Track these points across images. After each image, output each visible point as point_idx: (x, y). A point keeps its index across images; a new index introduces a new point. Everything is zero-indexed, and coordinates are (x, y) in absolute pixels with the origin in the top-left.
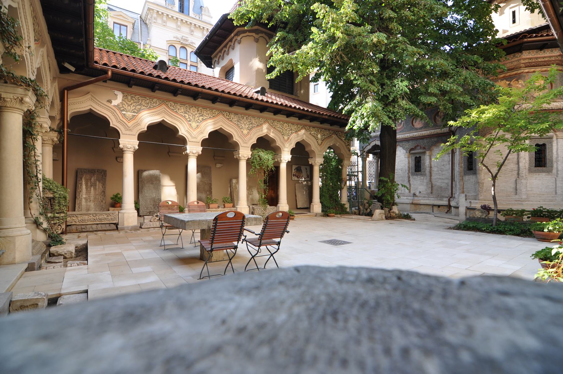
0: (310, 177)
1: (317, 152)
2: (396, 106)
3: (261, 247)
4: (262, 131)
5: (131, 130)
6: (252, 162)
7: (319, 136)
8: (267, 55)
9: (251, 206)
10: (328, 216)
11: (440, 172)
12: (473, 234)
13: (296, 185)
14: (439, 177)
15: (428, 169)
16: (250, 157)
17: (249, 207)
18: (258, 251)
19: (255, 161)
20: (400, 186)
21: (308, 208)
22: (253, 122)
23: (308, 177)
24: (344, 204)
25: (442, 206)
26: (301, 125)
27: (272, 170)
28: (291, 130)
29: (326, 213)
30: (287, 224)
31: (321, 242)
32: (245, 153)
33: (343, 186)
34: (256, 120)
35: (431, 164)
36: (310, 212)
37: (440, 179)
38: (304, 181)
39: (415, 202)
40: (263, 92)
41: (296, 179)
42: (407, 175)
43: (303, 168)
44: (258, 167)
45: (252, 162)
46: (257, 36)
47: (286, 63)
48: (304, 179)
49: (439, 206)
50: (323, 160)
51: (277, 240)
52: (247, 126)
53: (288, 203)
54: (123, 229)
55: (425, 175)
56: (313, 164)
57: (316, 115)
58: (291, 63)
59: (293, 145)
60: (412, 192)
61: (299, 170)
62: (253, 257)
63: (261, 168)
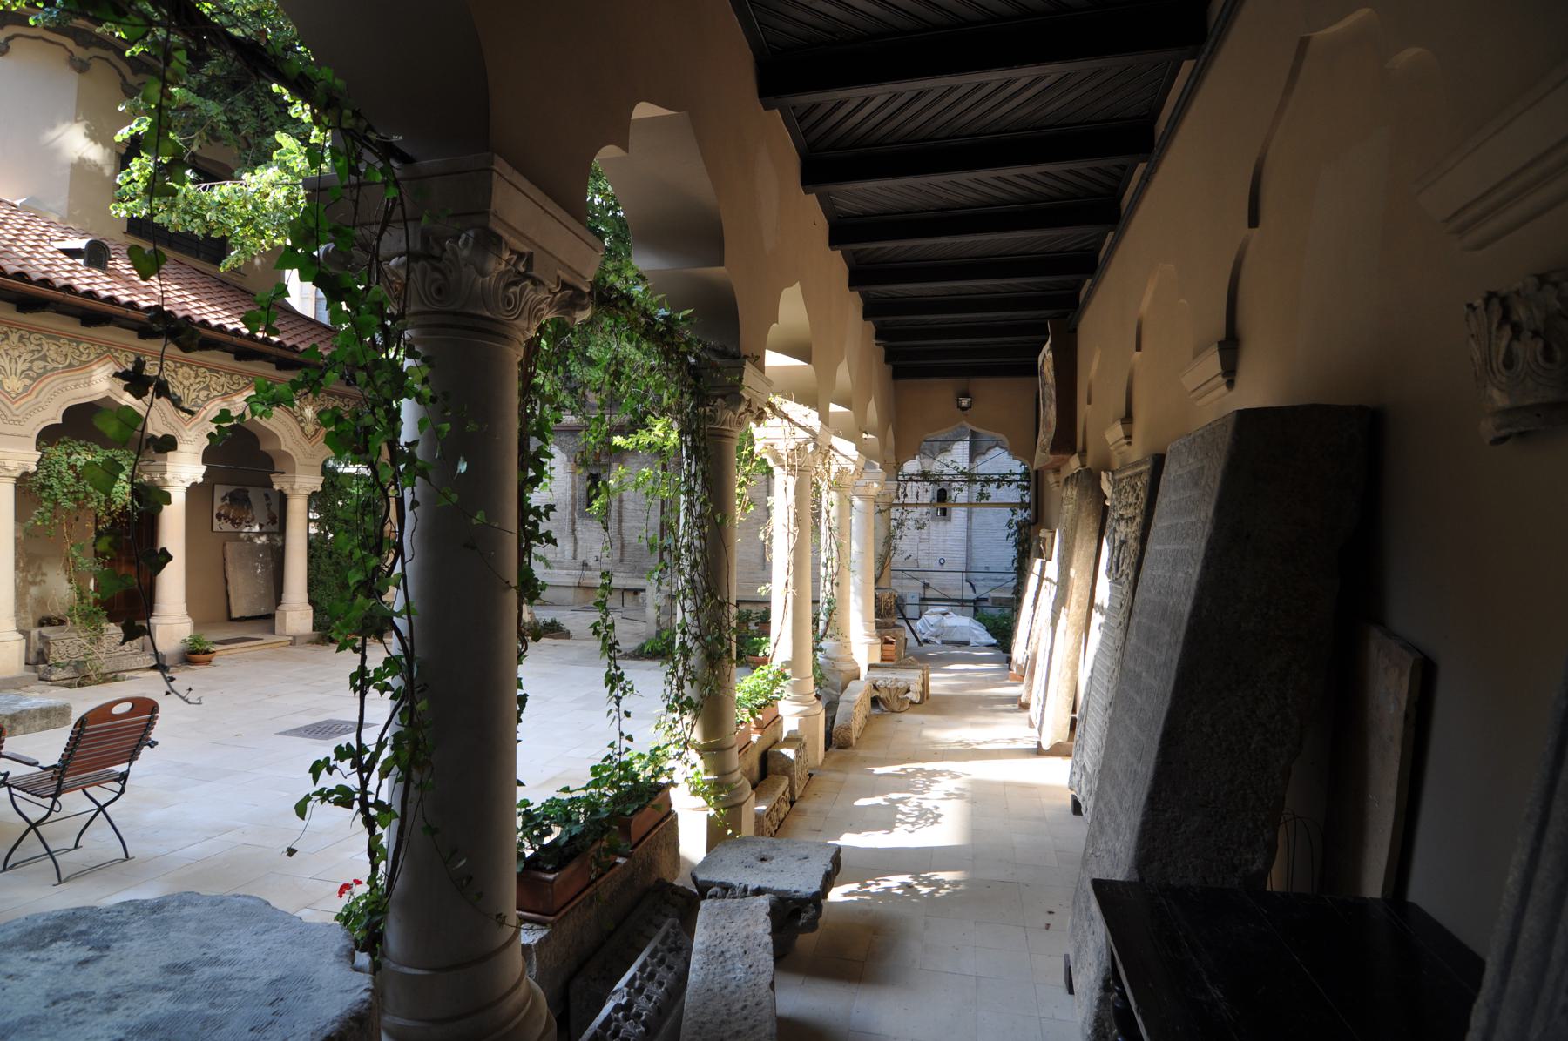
0: (278, 522)
1: (298, 456)
3: (63, 798)
4: (89, 384)
6: (42, 487)
8: (118, 138)
9: (35, 632)
12: (655, 668)
13: (231, 548)
16: (33, 468)
17: (25, 633)
18: (51, 810)
19: (55, 483)
21: (266, 619)
22: (52, 354)
23: (273, 521)
26: (243, 374)
27: (124, 512)
28: (207, 388)
29: (325, 632)
30: (150, 724)
31: (284, 733)
34: (65, 349)
36: (273, 632)
38: (260, 534)
39: (586, 582)
40: (96, 255)
41: (227, 527)
42: (568, 517)
43: (255, 495)
44: (69, 504)
45: (42, 487)
46: (80, 53)
47: (185, 212)
48: (257, 528)
51: (121, 768)
52: (22, 366)
53: (191, 611)
56: (288, 491)
57: (296, 356)
58: (203, 217)
60: (580, 558)
61: (238, 500)
62: (33, 826)
63: (81, 507)
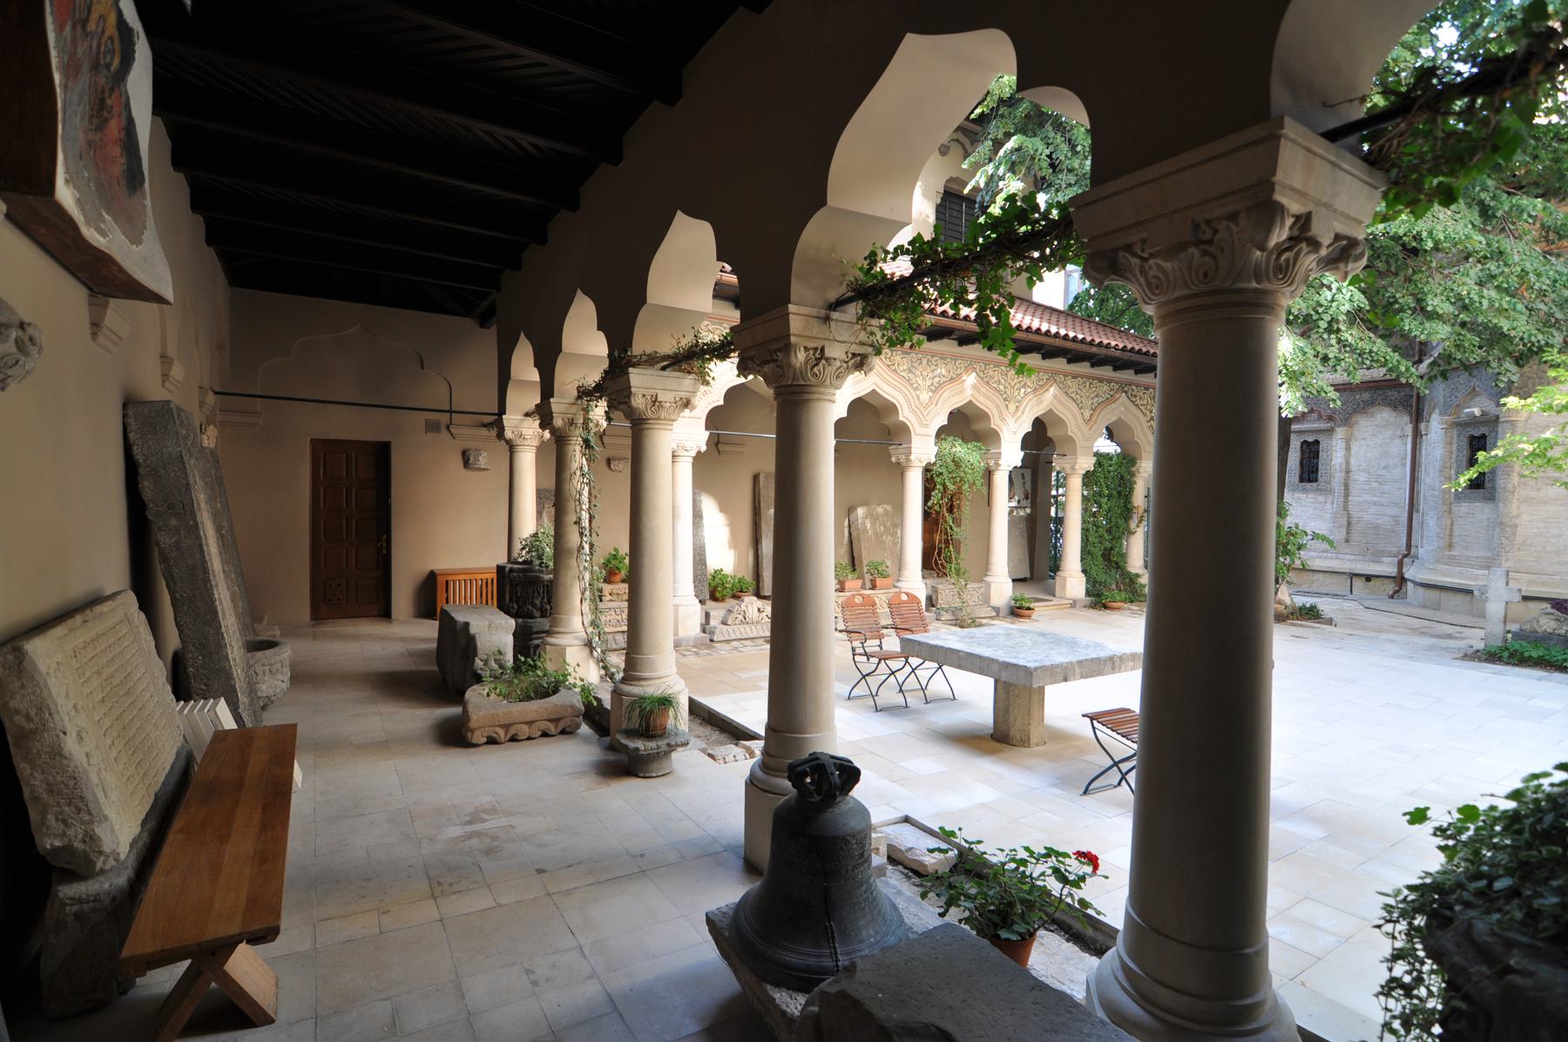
10: (1105, 607)
14: (1370, 498)
15: (1338, 477)
24: (1138, 576)
26: (1045, 371)
32: (923, 449)
33: (1133, 525)
35: (1348, 463)
37: (1375, 504)
49: (1368, 578)
50: (1094, 460)
55: (1329, 491)
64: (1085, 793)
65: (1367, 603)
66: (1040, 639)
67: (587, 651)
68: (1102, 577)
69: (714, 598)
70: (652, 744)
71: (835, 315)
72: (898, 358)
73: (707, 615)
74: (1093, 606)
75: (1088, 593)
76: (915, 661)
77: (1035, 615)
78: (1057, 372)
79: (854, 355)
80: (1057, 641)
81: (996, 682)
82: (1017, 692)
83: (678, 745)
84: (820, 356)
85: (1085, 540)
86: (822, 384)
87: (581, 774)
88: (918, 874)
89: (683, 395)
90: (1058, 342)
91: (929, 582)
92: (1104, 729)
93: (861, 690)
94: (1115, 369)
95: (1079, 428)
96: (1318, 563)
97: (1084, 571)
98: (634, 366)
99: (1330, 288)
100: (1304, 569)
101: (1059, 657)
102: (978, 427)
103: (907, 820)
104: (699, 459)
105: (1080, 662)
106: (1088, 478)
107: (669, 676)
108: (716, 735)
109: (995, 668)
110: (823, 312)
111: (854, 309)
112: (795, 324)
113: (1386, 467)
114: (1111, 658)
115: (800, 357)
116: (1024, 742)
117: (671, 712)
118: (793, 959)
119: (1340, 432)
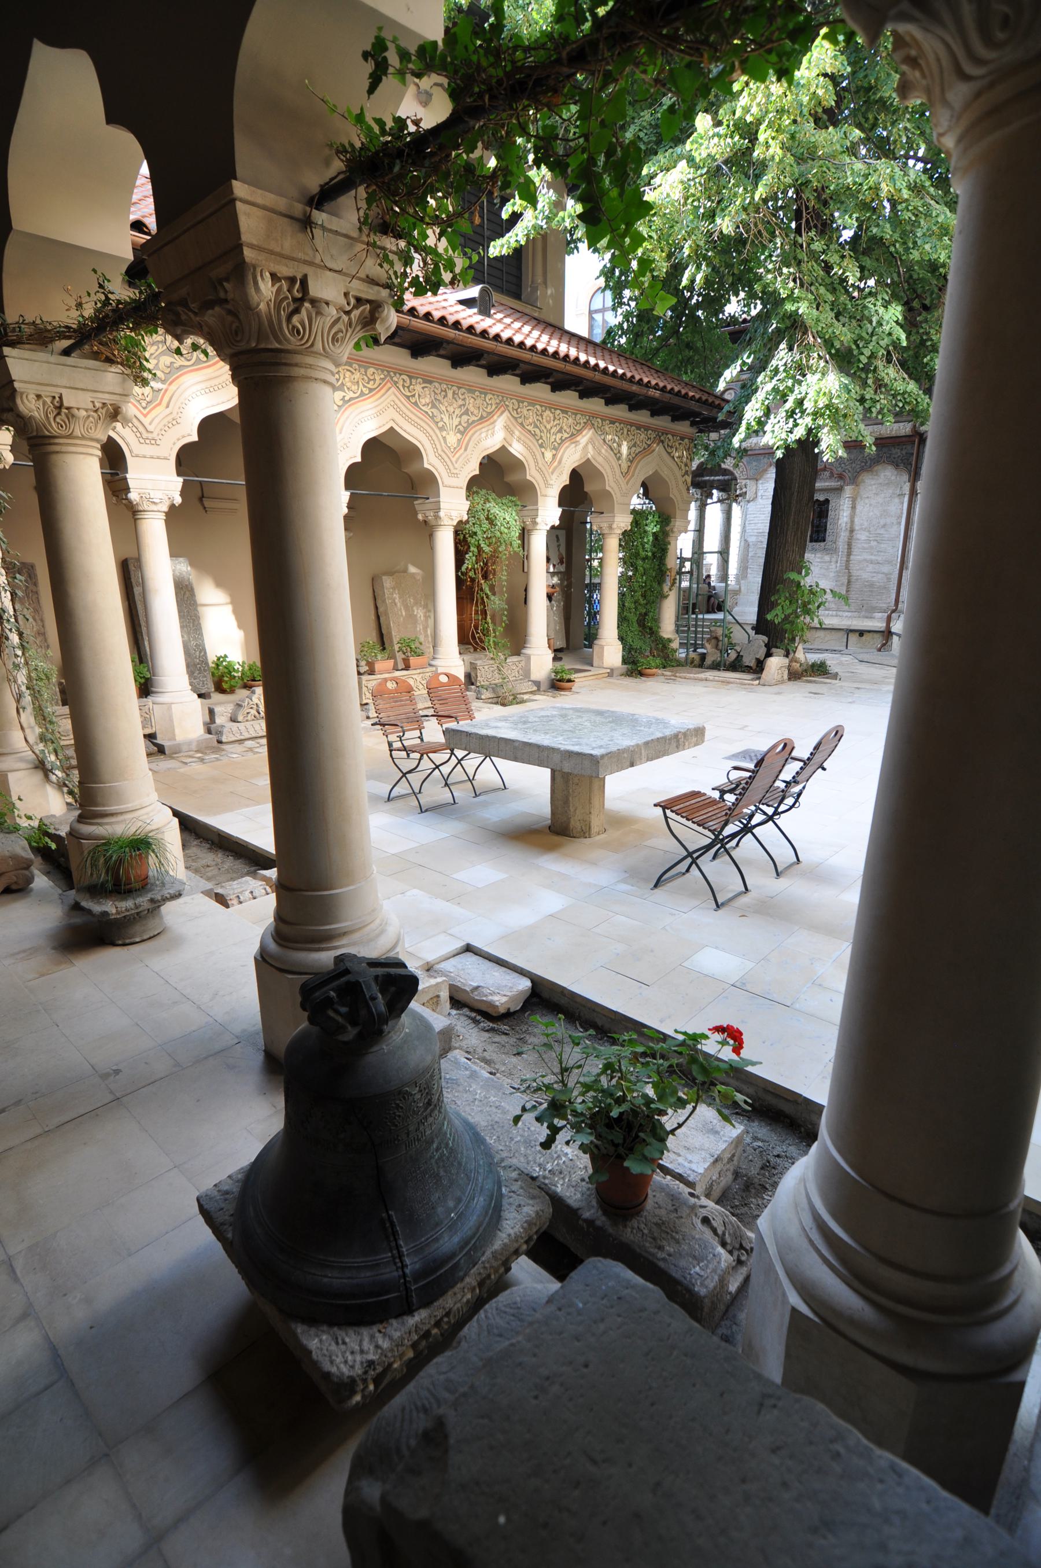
1: (617, 496)
2: (870, 382)
5: (154, 442)
7: (624, 449)
10: (641, 674)
11: (874, 544)
15: (843, 536)
16: (465, 518)
20: (829, 596)
23: (561, 562)
24: (670, 640)
25: (869, 631)
29: (634, 666)
32: (453, 505)
33: (666, 588)
35: (852, 522)
37: (872, 562)
49: (861, 633)
50: (630, 519)
52: (456, 421)
54: (177, 750)
55: (834, 551)
59: (565, 480)
64: (656, 886)
65: (860, 657)
66: (598, 719)
67: (39, 776)
68: (637, 644)
69: (220, 689)
70: (127, 905)
71: (320, 217)
72: (418, 388)
73: (211, 712)
74: (630, 674)
75: (625, 661)
76: (460, 753)
77: (575, 687)
78: (593, 416)
79: (359, 301)
80: (617, 720)
81: (553, 772)
82: (576, 780)
83: (165, 900)
84: (299, 294)
85: (622, 606)
86: (310, 350)
87: (32, 952)
88: (487, 1015)
89: (108, 398)
90: (598, 377)
91: (468, 658)
92: (678, 818)
93: (402, 789)
94: (654, 414)
95: (617, 482)
96: (830, 621)
97: (621, 638)
98: (13, 344)
99: (871, 322)
100: (821, 628)
101: (624, 740)
102: (512, 478)
103: (468, 949)
104: (173, 516)
105: (647, 743)
106: (628, 539)
107: (144, 805)
108: (229, 862)
109: (556, 758)
110: (299, 209)
111: (349, 213)
112: (251, 224)
113: (884, 526)
114: (676, 736)
115: (265, 292)
116: (585, 833)
117: (152, 860)
118: (333, 1279)
119: (848, 490)
